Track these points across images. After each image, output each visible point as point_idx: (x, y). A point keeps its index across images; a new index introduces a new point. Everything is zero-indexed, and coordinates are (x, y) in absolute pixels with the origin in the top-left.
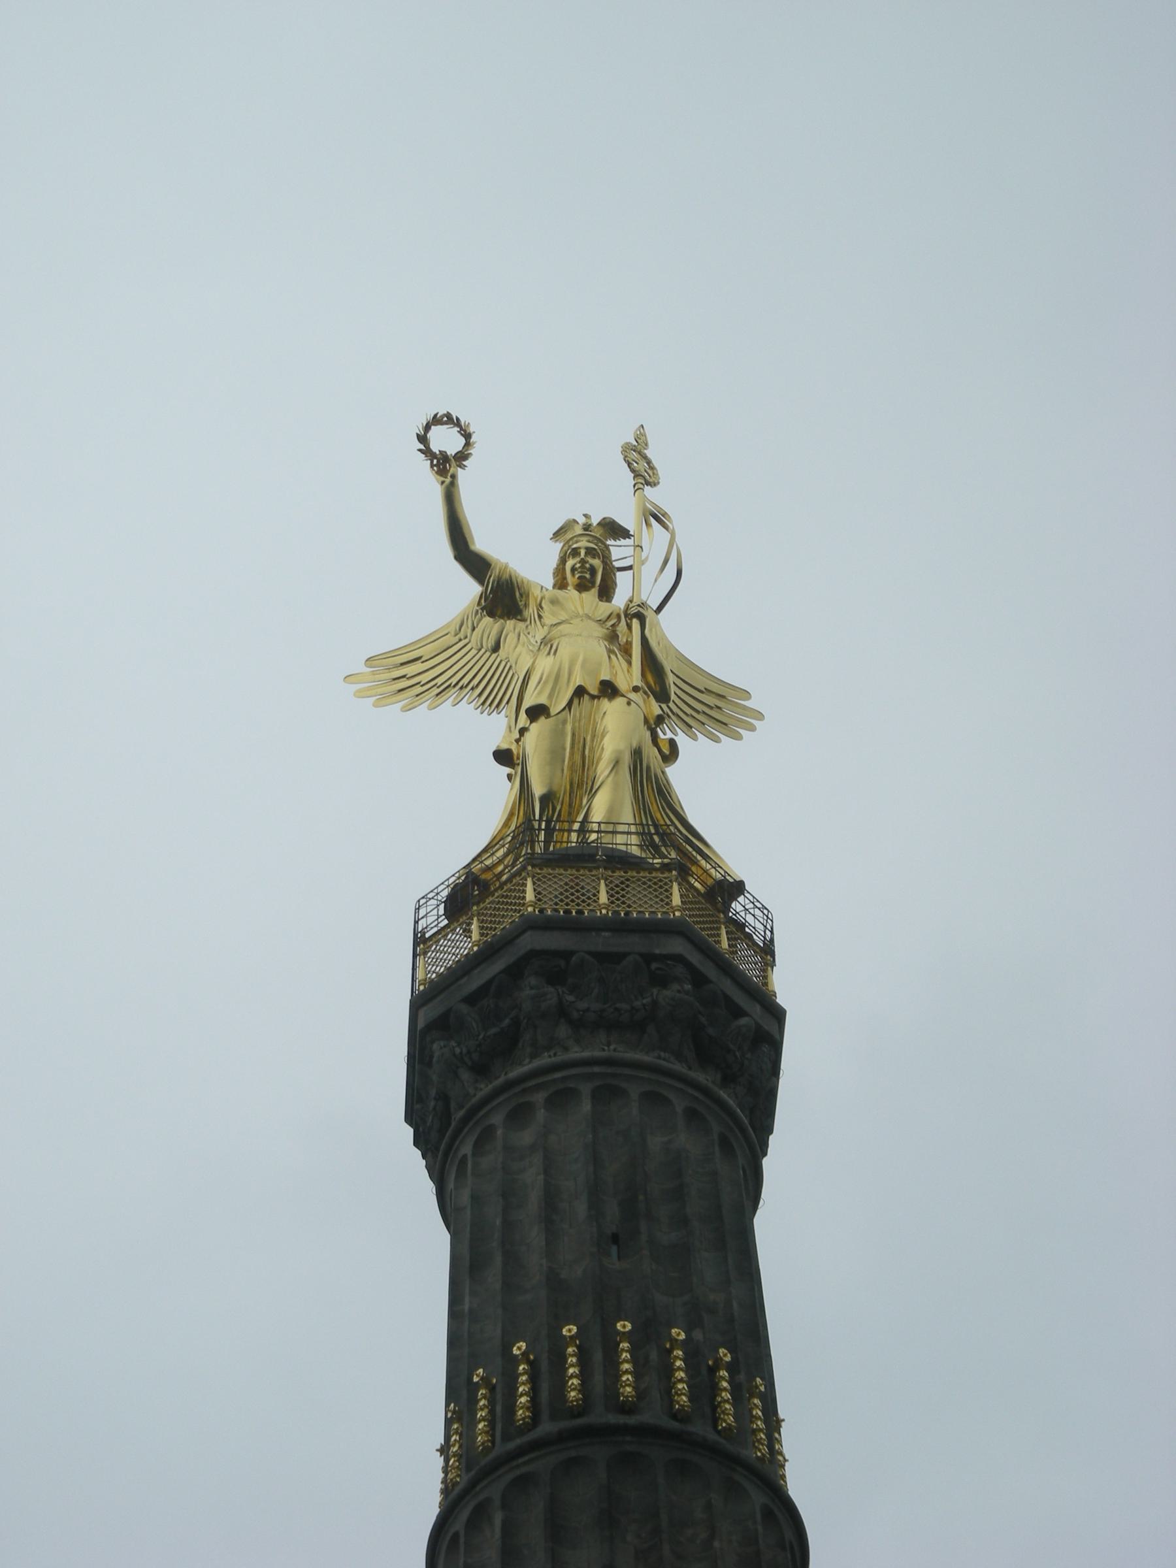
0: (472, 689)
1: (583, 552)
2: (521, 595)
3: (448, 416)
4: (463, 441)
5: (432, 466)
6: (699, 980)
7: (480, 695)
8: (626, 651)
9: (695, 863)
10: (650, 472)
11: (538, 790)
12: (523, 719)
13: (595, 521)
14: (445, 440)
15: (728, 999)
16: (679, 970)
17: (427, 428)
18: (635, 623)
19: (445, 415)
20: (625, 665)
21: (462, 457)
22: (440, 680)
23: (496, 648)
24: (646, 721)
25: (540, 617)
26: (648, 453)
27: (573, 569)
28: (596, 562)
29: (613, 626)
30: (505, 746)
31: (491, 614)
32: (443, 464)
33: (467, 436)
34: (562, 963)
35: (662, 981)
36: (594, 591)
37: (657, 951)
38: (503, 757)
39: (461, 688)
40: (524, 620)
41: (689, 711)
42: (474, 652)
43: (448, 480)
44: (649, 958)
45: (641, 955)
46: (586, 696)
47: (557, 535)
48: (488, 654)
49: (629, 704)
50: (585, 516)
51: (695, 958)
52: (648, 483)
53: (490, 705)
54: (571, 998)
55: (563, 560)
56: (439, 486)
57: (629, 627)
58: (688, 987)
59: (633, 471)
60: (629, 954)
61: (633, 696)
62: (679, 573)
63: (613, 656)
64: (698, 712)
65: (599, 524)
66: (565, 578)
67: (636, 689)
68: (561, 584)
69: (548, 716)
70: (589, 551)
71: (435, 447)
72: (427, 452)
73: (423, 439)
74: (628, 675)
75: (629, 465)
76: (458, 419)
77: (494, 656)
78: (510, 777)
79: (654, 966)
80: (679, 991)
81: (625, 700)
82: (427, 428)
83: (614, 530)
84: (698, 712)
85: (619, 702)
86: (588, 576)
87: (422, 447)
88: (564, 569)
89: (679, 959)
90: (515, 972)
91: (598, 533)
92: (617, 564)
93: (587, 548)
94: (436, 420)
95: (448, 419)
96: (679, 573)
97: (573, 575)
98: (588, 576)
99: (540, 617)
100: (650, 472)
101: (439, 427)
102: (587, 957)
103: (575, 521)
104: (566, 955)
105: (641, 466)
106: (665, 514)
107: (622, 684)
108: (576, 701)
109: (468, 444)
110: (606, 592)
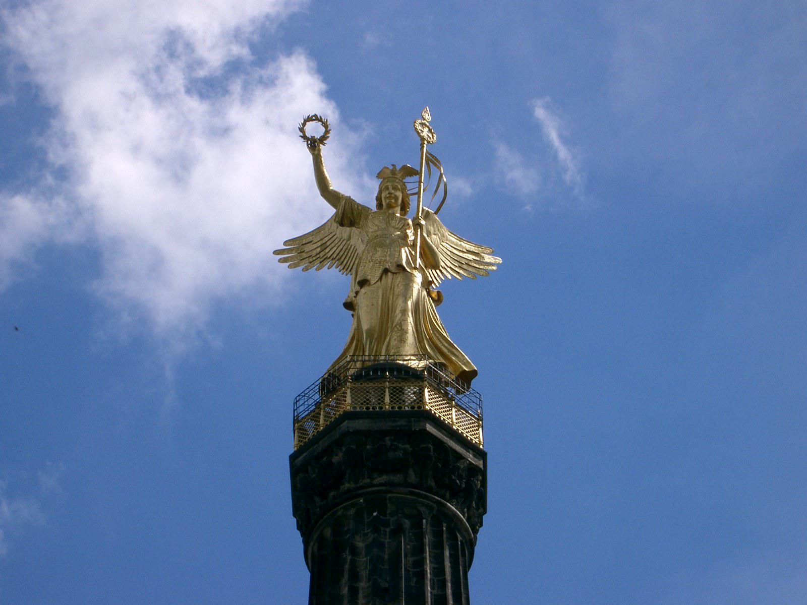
3: (315, 116)
4: (323, 129)
5: (308, 145)
11: (365, 326)
12: (358, 288)
17: (304, 124)
19: (312, 116)
21: (323, 139)
30: (349, 300)
31: (342, 225)
32: (314, 145)
39: (332, 259)
50: (392, 165)
55: (380, 192)
68: (380, 205)
71: (308, 135)
73: (302, 130)
77: (349, 242)
78: (353, 315)
82: (304, 124)
87: (301, 134)
92: (409, 192)
94: (309, 119)
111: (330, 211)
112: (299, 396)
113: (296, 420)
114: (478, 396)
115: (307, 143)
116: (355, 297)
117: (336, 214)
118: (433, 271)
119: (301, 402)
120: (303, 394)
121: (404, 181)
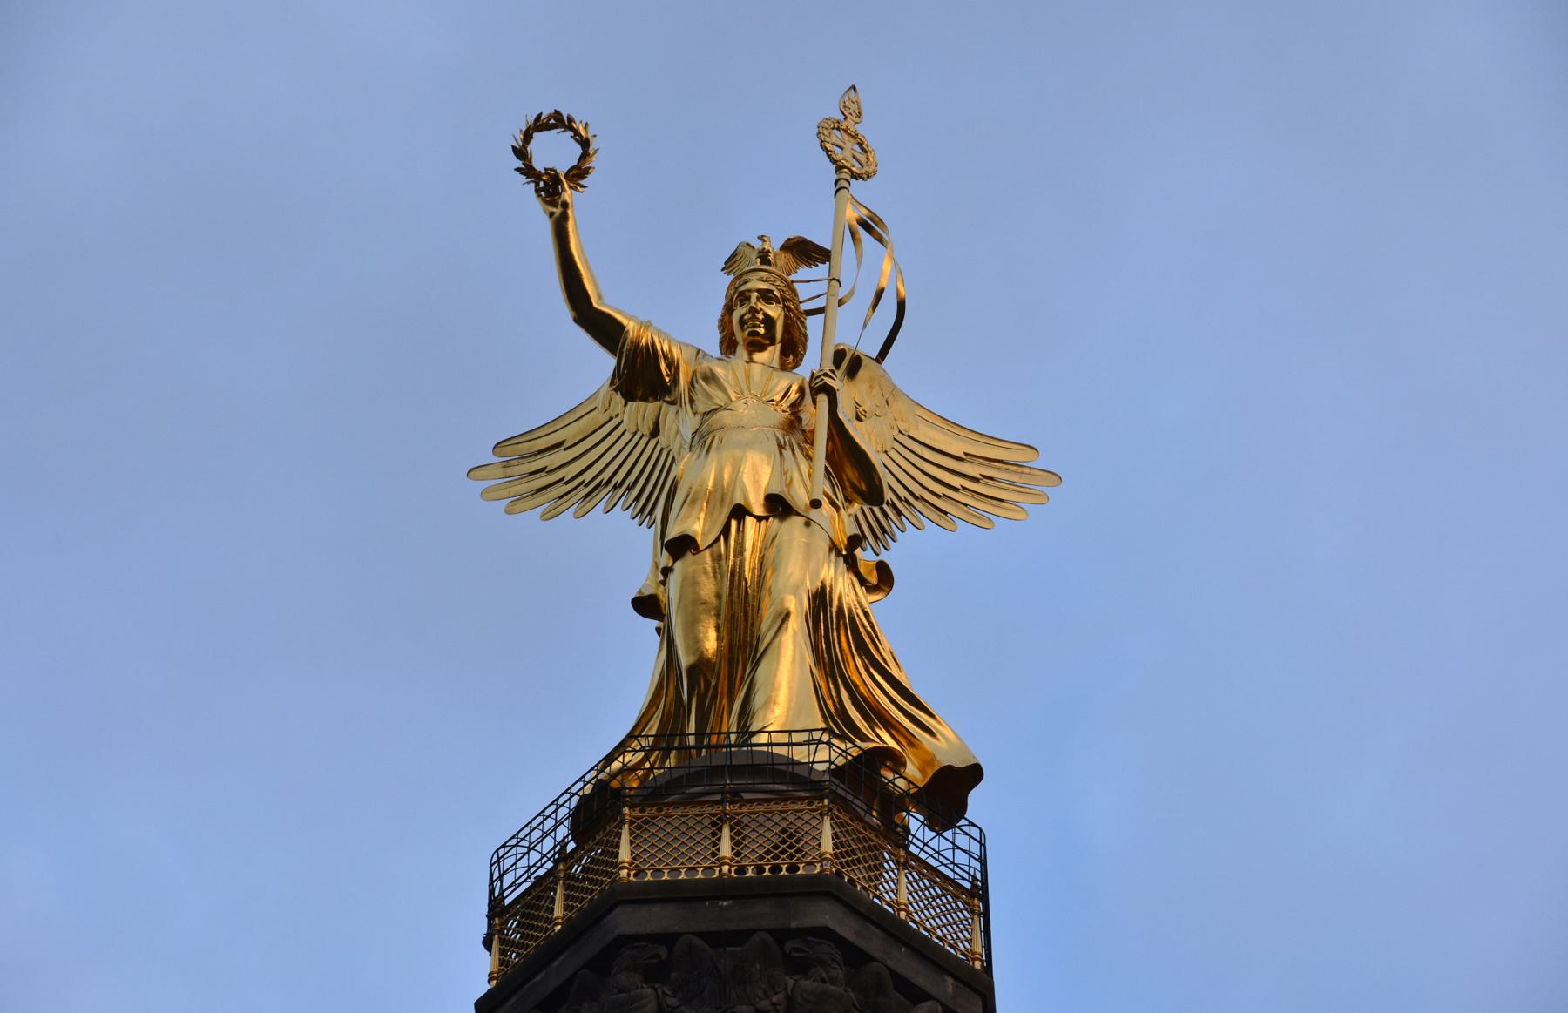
2: (669, 366)
3: (557, 115)
4: (578, 150)
5: (538, 191)
6: (854, 957)
7: (637, 498)
8: (809, 438)
9: (912, 742)
10: (862, 158)
11: (685, 660)
12: (665, 559)
13: (774, 245)
14: (553, 152)
15: (902, 983)
16: (826, 950)
17: (527, 137)
18: (823, 399)
19: (550, 117)
20: (804, 466)
21: (578, 174)
22: (588, 476)
23: (655, 432)
24: (834, 547)
25: (692, 401)
26: (861, 129)
27: (742, 322)
28: (774, 311)
31: (629, 396)
32: (550, 187)
33: (585, 143)
34: (663, 952)
35: (800, 966)
36: (770, 355)
37: (794, 925)
38: (647, 606)
39: (615, 487)
40: (673, 403)
43: (558, 211)
44: (782, 935)
45: (770, 931)
46: (749, 520)
47: (730, 263)
49: (807, 524)
50: (761, 238)
51: (847, 928)
54: (672, 1001)
55: (729, 309)
56: (547, 218)
57: (814, 402)
58: (839, 973)
59: (834, 161)
60: (753, 932)
61: (813, 514)
62: (901, 305)
63: (787, 453)
64: (955, 489)
65: (783, 248)
66: (733, 334)
68: (728, 346)
69: (697, 550)
70: (766, 296)
71: (539, 164)
72: (528, 171)
73: (521, 153)
74: (807, 479)
75: (827, 151)
76: (570, 120)
77: (653, 442)
78: (658, 630)
79: (789, 945)
80: (823, 981)
82: (527, 137)
83: (805, 251)
84: (955, 489)
85: (797, 522)
86: (762, 331)
87: (520, 164)
88: (731, 321)
89: (825, 933)
90: (602, 965)
91: (784, 260)
92: (803, 307)
93: (759, 291)
94: (539, 125)
95: (559, 121)
96: (901, 305)
97: (743, 330)
98: (762, 331)
99: (692, 401)
100: (862, 158)
101: (545, 133)
102: (697, 941)
104: (668, 939)
106: (880, 222)
107: (800, 496)
108: (734, 523)
109: (585, 156)
111: (605, 363)
112: (504, 846)
113: (496, 908)
114: (975, 832)
115: (537, 185)
116: (664, 583)
118: (866, 508)
119: (508, 862)
120: (514, 842)
121: (792, 278)
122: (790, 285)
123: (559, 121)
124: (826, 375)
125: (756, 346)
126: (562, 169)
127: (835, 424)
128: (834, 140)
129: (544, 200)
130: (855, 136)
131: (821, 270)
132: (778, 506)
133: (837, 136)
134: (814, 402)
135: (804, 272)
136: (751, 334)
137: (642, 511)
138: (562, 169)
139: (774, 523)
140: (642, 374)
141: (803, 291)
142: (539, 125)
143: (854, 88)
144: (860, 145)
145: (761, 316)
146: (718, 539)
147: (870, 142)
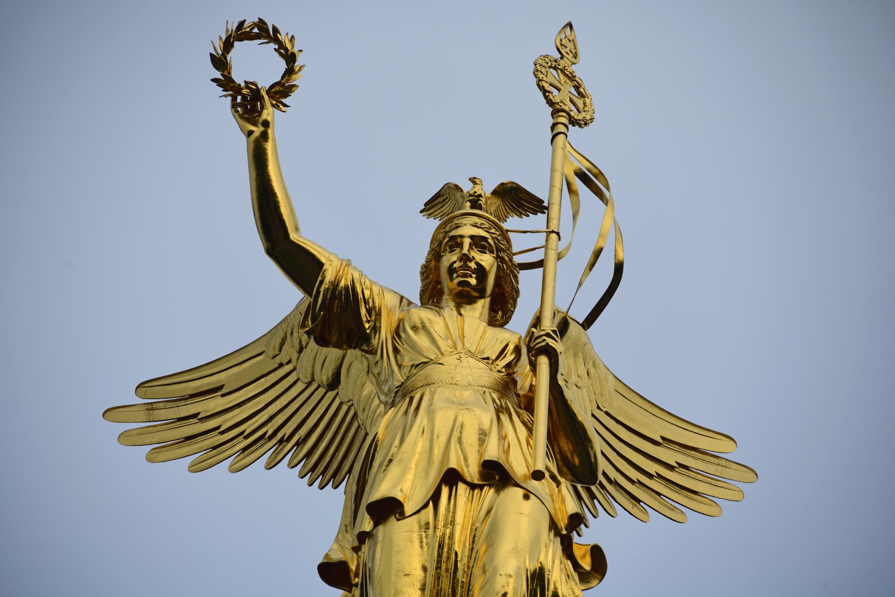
0: (297, 444)
1: (467, 242)
2: (369, 311)
3: (261, 24)
4: (282, 65)
5: (234, 106)
7: (308, 455)
13: (486, 189)
14: (256, 65)
17: (228, 45)
21: (281, 91)
22: (248, 427)
26: (578, 70)
27: (451, 270)
28: (487, 260)
29: (508, 366)
31: (323, 342)
32: (249, 104)
33: (290, 58)
40: (373, 352)
41: (634, 475)
42: (300, 386)
43: (257, 130)
47: (431, 206)
48: (322, 391)
49: (526, 497)
50: (473, 180)
52: (574, 122)
53: (323, 473)
55: (436, 254)
59: (551, 103)
65: (495, 193)
67: (537, 475)
68: (432, 294)
69: (402, 516)
71: (239, 76)
72: (226, 83)
73: (220, 62)
76: (276, 30)
77: (331, 394)
81: (520, 492)
82: (228, 45)
83: (515, 198)
85: (514, 494)
87: (218, 75)
88: (437, 268)
92: (518, 259)
95: (263, 32)
97: (452, 279)
103: (457, 187)
105: (564, 95)
108: (445, 491)
109: (290, 71)
110: (501, 307)
115: (234, 99)
117: (311, 308)
121: (505, 226)
122: (504, 233)
123: (263, 32)
124: (548, 335)
125: (464, 298)
126: (264, 84)
127: (556, 391)
128: (550, 79)
129: (241, 116)
130: (572, 78)
131: (537, 221)
132: (496, 475)
133: (553, 76)
134: (533, 366)
135: (513, 222)
136: (460, 284)
137: (313, 470)
138: (264, 84)
139: (489, 493)
140: (337, 317)
141: (518, 243)
142: (241, 33)
143: (570, 25)
144: (577, 88)
145: (473, 265)
146: (426, 506)
147: (588, 87)
